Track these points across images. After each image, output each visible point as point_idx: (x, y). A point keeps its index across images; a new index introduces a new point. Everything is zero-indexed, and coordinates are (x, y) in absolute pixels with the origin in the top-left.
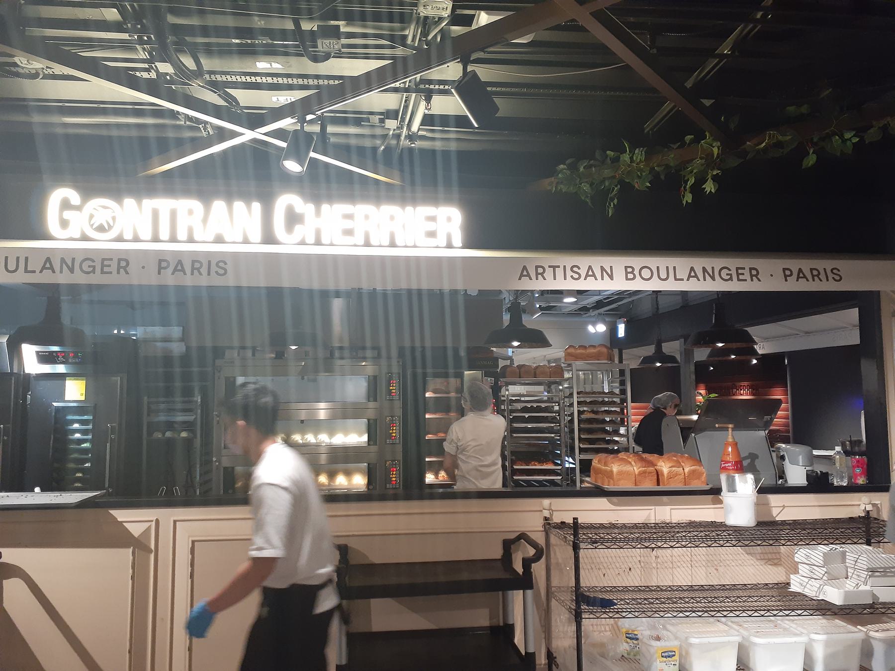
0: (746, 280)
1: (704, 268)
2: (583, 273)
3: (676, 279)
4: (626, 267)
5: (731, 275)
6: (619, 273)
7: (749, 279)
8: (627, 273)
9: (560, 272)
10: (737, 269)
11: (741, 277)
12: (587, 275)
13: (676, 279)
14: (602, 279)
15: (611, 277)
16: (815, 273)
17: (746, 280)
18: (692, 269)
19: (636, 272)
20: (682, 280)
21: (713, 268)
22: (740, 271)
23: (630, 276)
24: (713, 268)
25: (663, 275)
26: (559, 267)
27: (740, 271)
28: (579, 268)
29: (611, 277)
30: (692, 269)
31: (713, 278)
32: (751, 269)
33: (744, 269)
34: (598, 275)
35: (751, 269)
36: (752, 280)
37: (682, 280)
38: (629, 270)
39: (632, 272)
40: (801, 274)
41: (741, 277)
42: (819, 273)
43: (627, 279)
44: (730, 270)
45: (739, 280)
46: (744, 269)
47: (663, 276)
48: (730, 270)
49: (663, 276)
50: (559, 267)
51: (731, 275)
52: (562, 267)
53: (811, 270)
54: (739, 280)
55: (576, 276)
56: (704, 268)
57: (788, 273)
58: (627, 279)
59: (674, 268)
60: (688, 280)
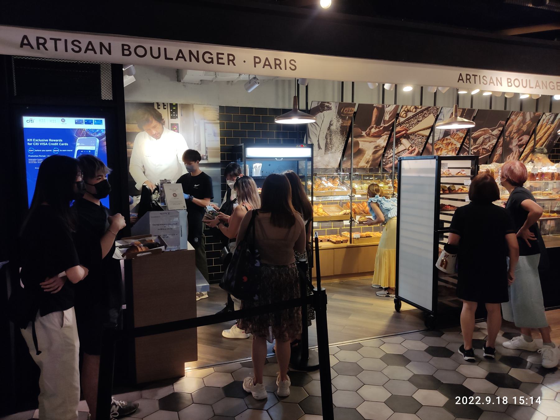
0: (223, 64)
1: (190, 51)
2: (83, 47)
3: (166, 58)
4: (123, 45)
5: (212, 58)
6: (505, 82)
7: (226, 63)
8: (123, 50)
9: (61, 45)
10: (218, 54)
11: (220, 61)
12: (87, 49)
13: (166, 58)
14: (191, 61)
15: (109, 52)
16: (278, 62)
17: (223, 64)
18: (180, 51)
19: (132, 50)
20: (172, 59)
21: (198, 52)
22: (220, 56)
23: (127, 52)
24: (198, 52)
25: (156, 54)
26: (60, 40)
27: (220, 56)
28: (80, 43)
29: (109, 52)
30: (180, 51)
31: (198, 60)
32: (229, 55)
33: (223, 54)
34: (187, 58)
35: (229, 55)
36: (229, 64)
37: (172, 59)
38: (126, 47)
39: (128, 50)
40: (267, 63)
41: (220, 61)
42: (280, 63)
43: (123, 54)
44: (211, 54)
45: (218, 63)
46: (223, 54)
47: (156, 54)
48: (211, 54)
49: (525, 85)
50: (60, 40)
51: (212, 58)
52: (63, 42)
53: (275, 59)
54: (218, 63)
55: (77, 49)
56: (190, 51)
57: (257, 60)
58: (123, 54)
59: (165, 49)
60: (177, 59)
